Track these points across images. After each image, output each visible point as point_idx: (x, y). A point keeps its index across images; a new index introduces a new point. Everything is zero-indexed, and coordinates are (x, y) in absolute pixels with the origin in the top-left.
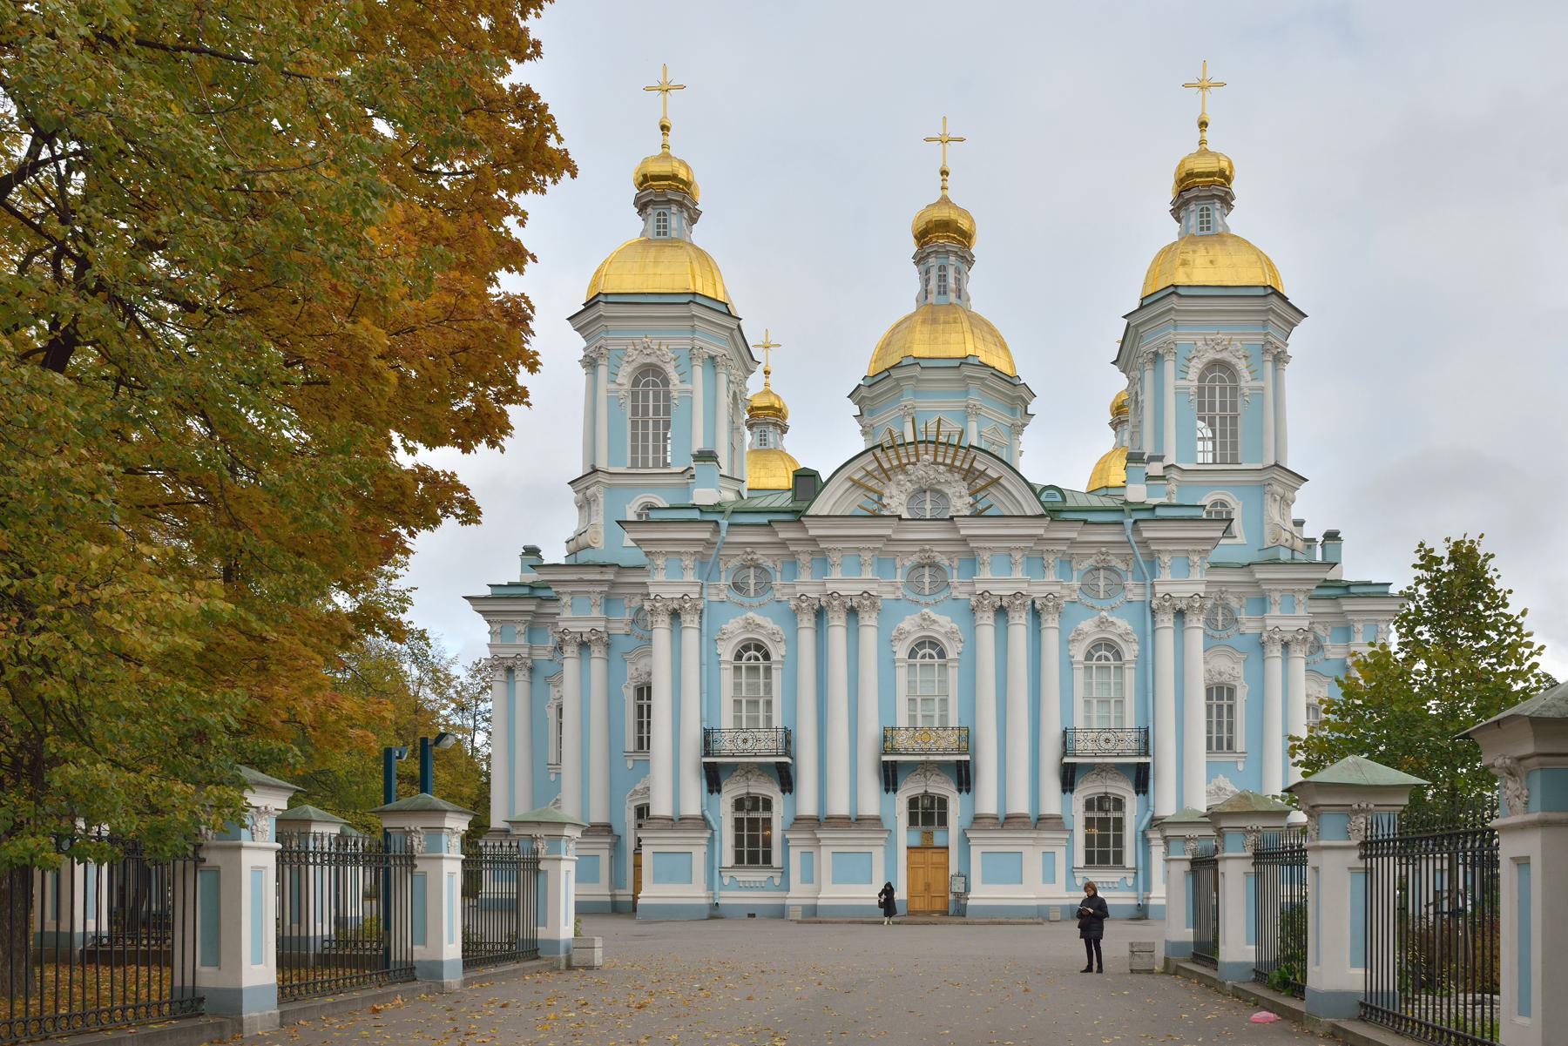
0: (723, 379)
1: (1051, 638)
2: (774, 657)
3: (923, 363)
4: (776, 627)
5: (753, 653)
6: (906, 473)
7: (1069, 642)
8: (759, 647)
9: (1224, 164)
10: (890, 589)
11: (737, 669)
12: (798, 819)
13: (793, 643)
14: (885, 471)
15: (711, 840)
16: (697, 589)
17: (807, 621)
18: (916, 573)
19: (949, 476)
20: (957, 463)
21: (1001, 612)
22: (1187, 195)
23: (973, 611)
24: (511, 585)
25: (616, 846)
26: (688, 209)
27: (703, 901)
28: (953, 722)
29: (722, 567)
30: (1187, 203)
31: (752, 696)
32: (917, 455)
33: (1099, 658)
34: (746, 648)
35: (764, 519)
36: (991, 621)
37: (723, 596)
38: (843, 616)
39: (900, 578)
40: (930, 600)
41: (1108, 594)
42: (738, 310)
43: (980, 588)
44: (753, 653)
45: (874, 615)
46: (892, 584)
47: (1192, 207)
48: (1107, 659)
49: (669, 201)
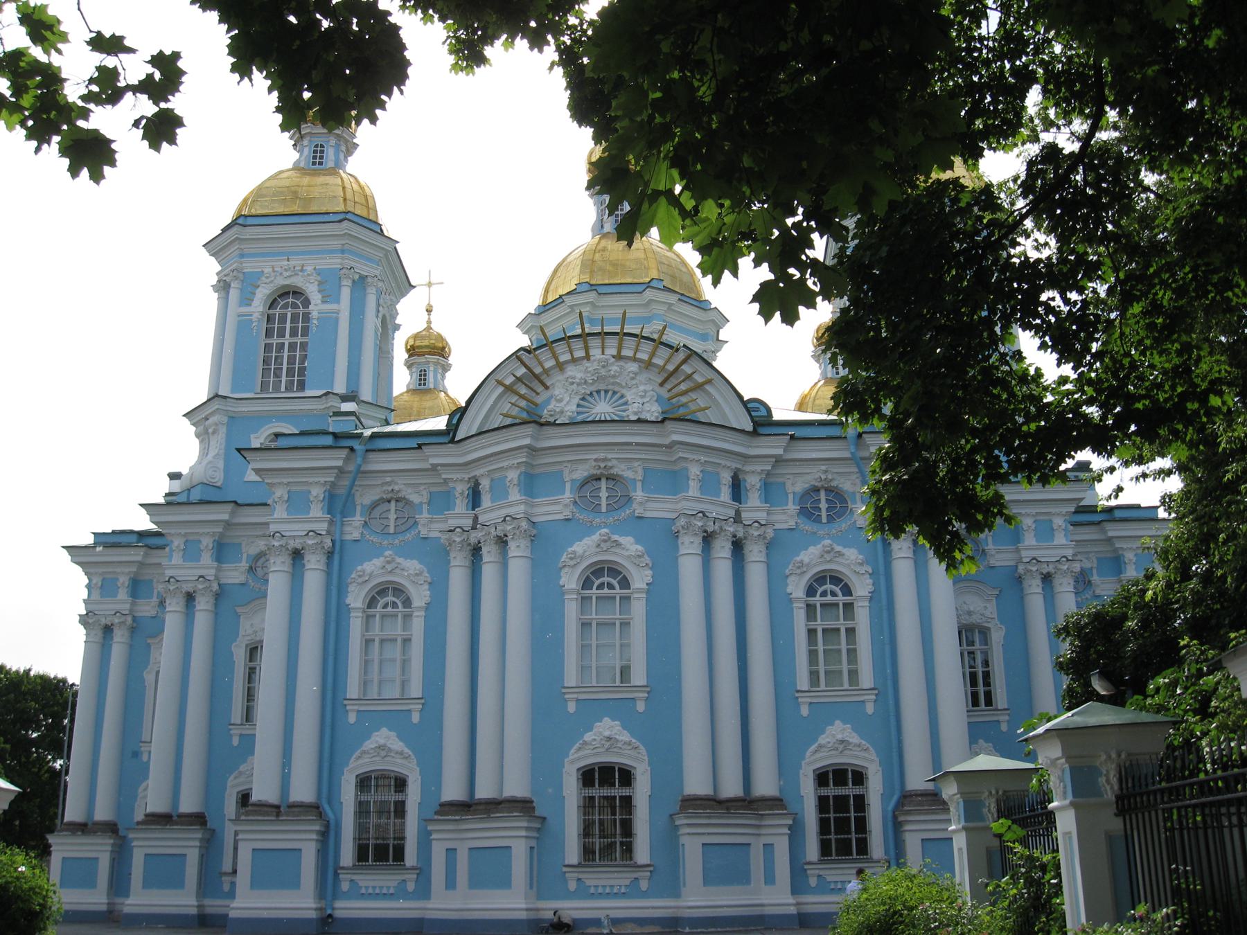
0: (371, 300)
3: (601, 290)
5: (390, 598)
8: (398, 590)
11: (368, 618)
12: (442, 805)
13: (439, 586)
15: (324, 835)
16: (325, 525)
24: (114, 532)
25: (210, 845)
26: (346, 141)
27: (313, 915)
33: (824, 594)
34: (382, 592)
35: (413, 443)
41: (831, 519)
42: (389, 230)
44: (390, 598)
48: (834, 594)
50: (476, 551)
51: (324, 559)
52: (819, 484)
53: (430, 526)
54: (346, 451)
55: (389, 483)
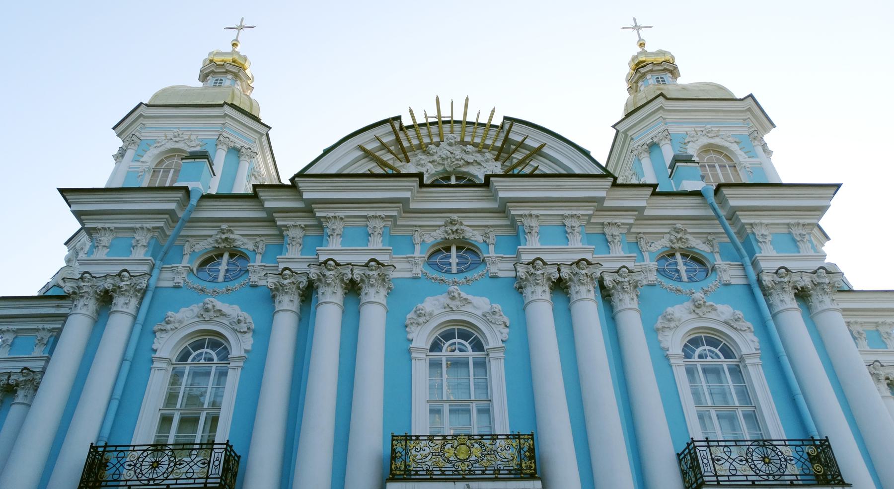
1: (632, 320)
2: (235, 352)
4: (244, 315)
6: (426, 153)
7: (657, 330)
9: (668, 57)
10: (408, 266)
13: (263, 336)
14: (403, 150)
17: (289, 303)
18: (437, 259)
19: (479, 157)
20: (489, 142)
21: (560, 286)
22: (643, 70)
23: (520, 289)
28: (502, 427)
29: (187, 248)
30: (644, 74)
31: (190, 412)
32: (440, 135)
36: (547, 296)
37: (179, 280)
38: (340, 292)
39: (420, 253)
40: (460, 278)
43: (527, 258)
45: (383, 292)
46: (408, 260)
47: (649, 76)
49: (227, 72)
50: (308, 293)
51: (134, 302)
52: (676, 246)
53: (260, 273)
54: (180, 195)
55: (223, 232)
